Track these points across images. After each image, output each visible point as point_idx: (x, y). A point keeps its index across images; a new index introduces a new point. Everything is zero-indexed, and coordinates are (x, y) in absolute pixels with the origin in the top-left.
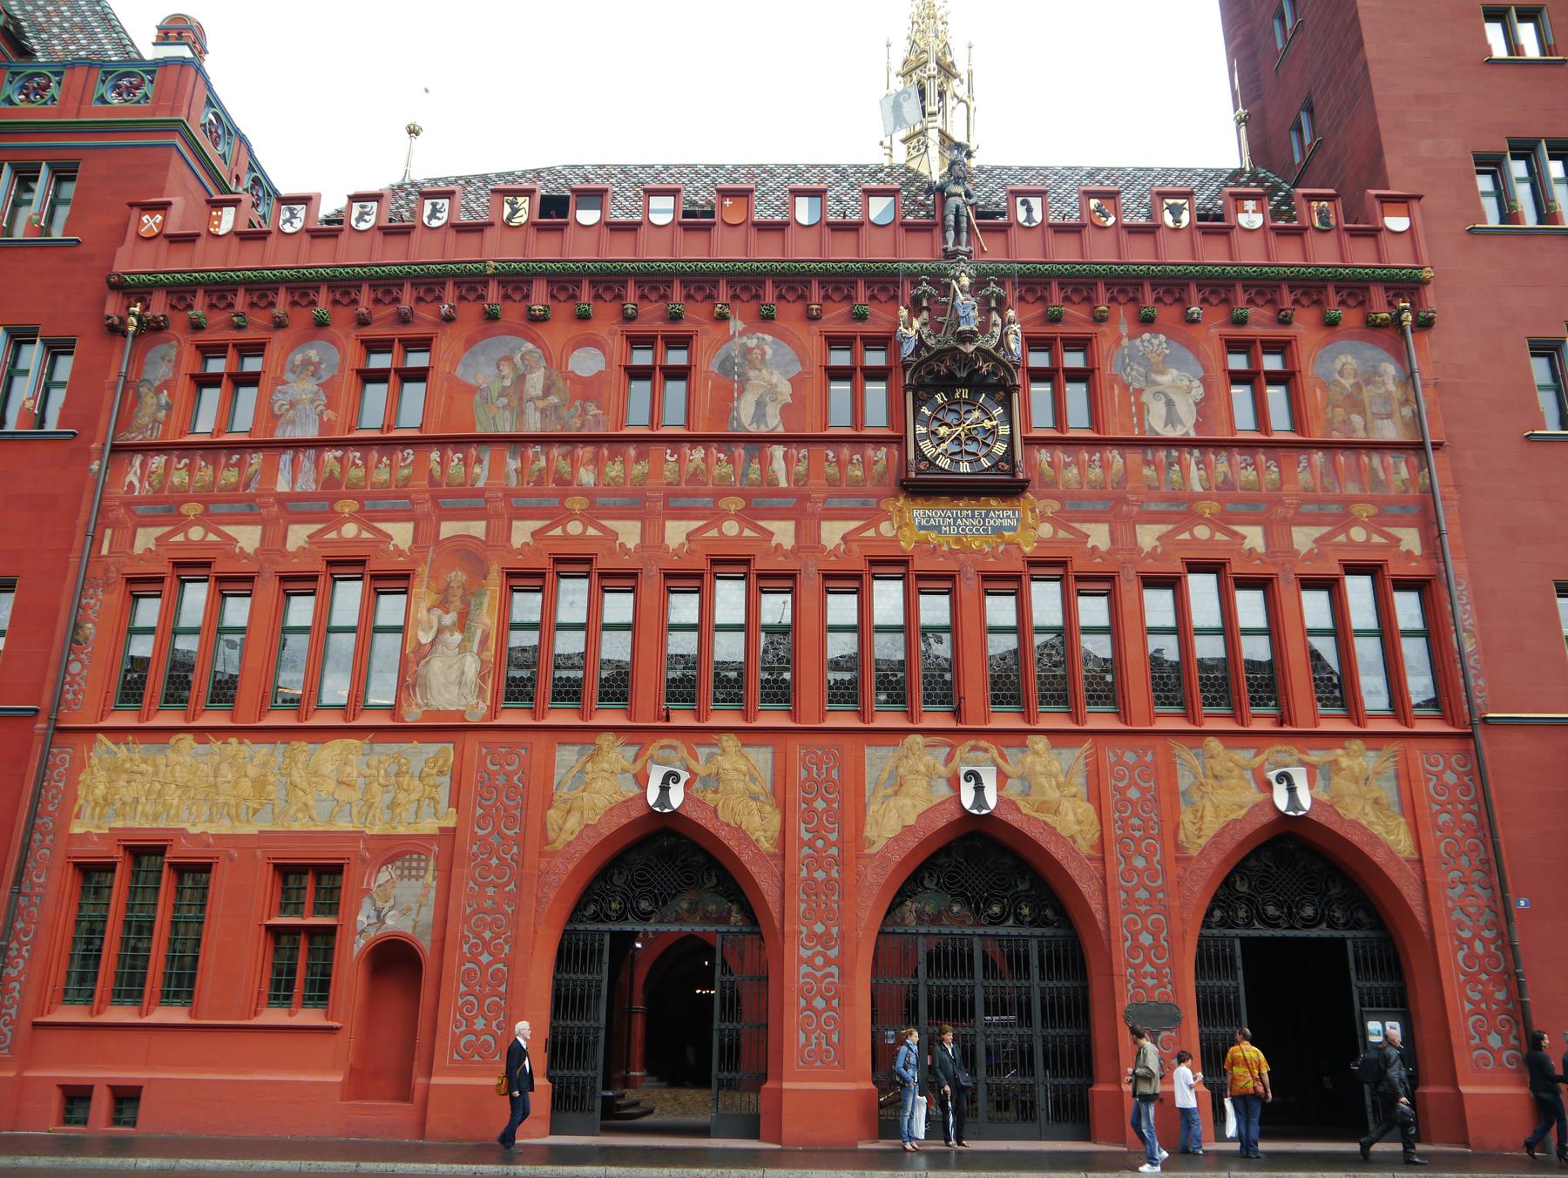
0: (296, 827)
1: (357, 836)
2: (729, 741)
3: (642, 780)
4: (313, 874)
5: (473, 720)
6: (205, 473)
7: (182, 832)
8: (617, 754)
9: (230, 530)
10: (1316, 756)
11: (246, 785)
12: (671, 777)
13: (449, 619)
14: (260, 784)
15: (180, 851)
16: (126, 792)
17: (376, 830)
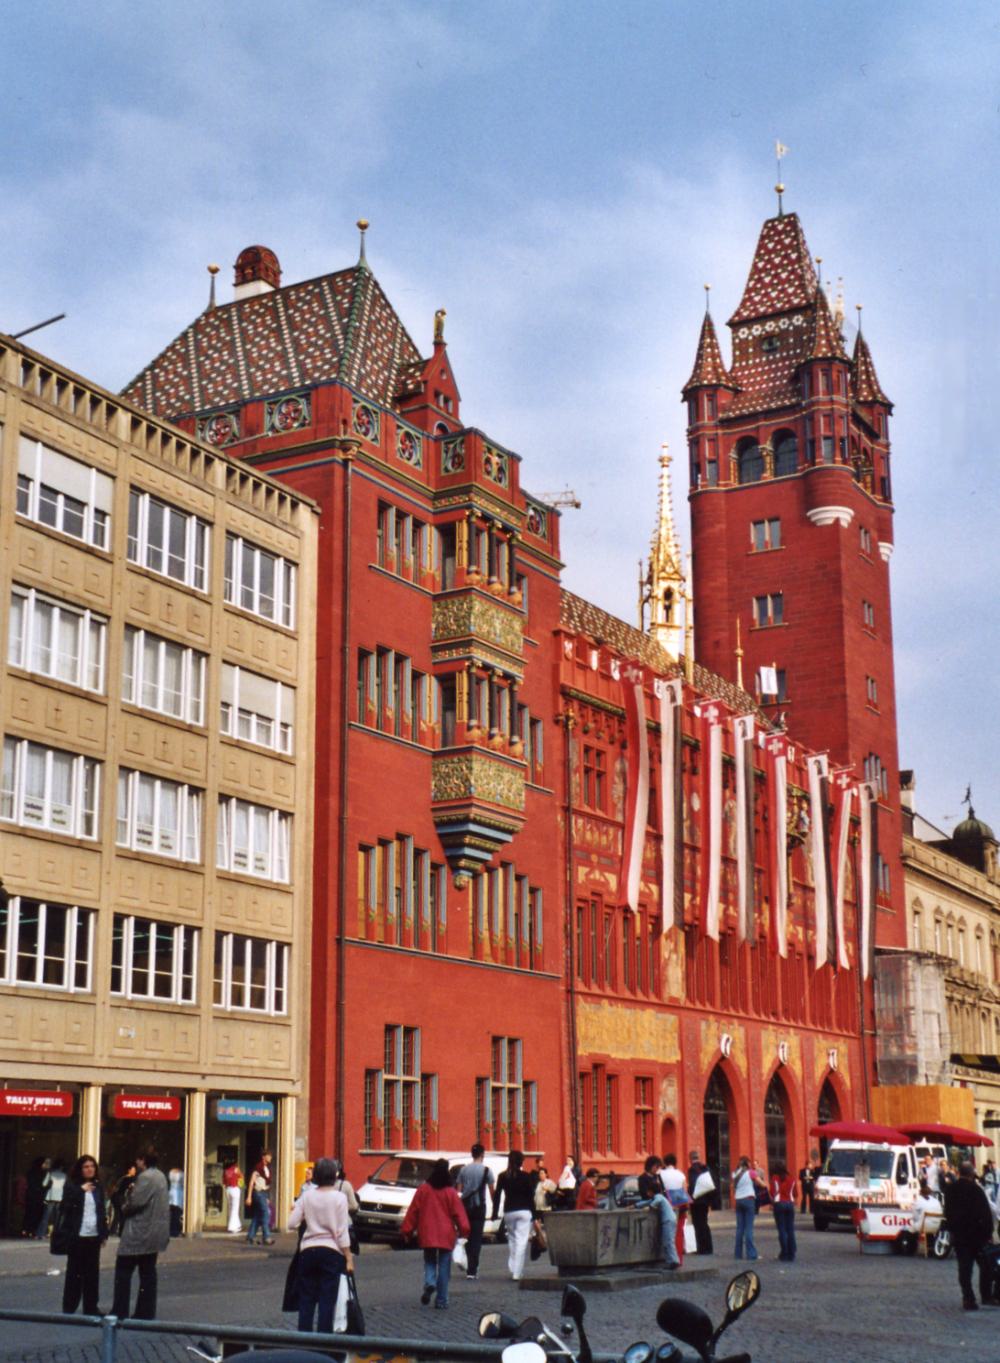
0: (641, 1056)
1: (653, 1063)
2: (735, 1022)
3: (719, 1040)
4: (646, 1081)
5: (682, 1004)
6: (596, 835)
7: (608, 1056)
8: (714, 1026)
9: (607, 874)
10: (836, 1045)
11: (625, 1031)
12: (728, 1040)
13: (672, 946)
14: (629, 1031)
15: (610, 1068)
16: (592, 1032)
17: (661, 1060)
